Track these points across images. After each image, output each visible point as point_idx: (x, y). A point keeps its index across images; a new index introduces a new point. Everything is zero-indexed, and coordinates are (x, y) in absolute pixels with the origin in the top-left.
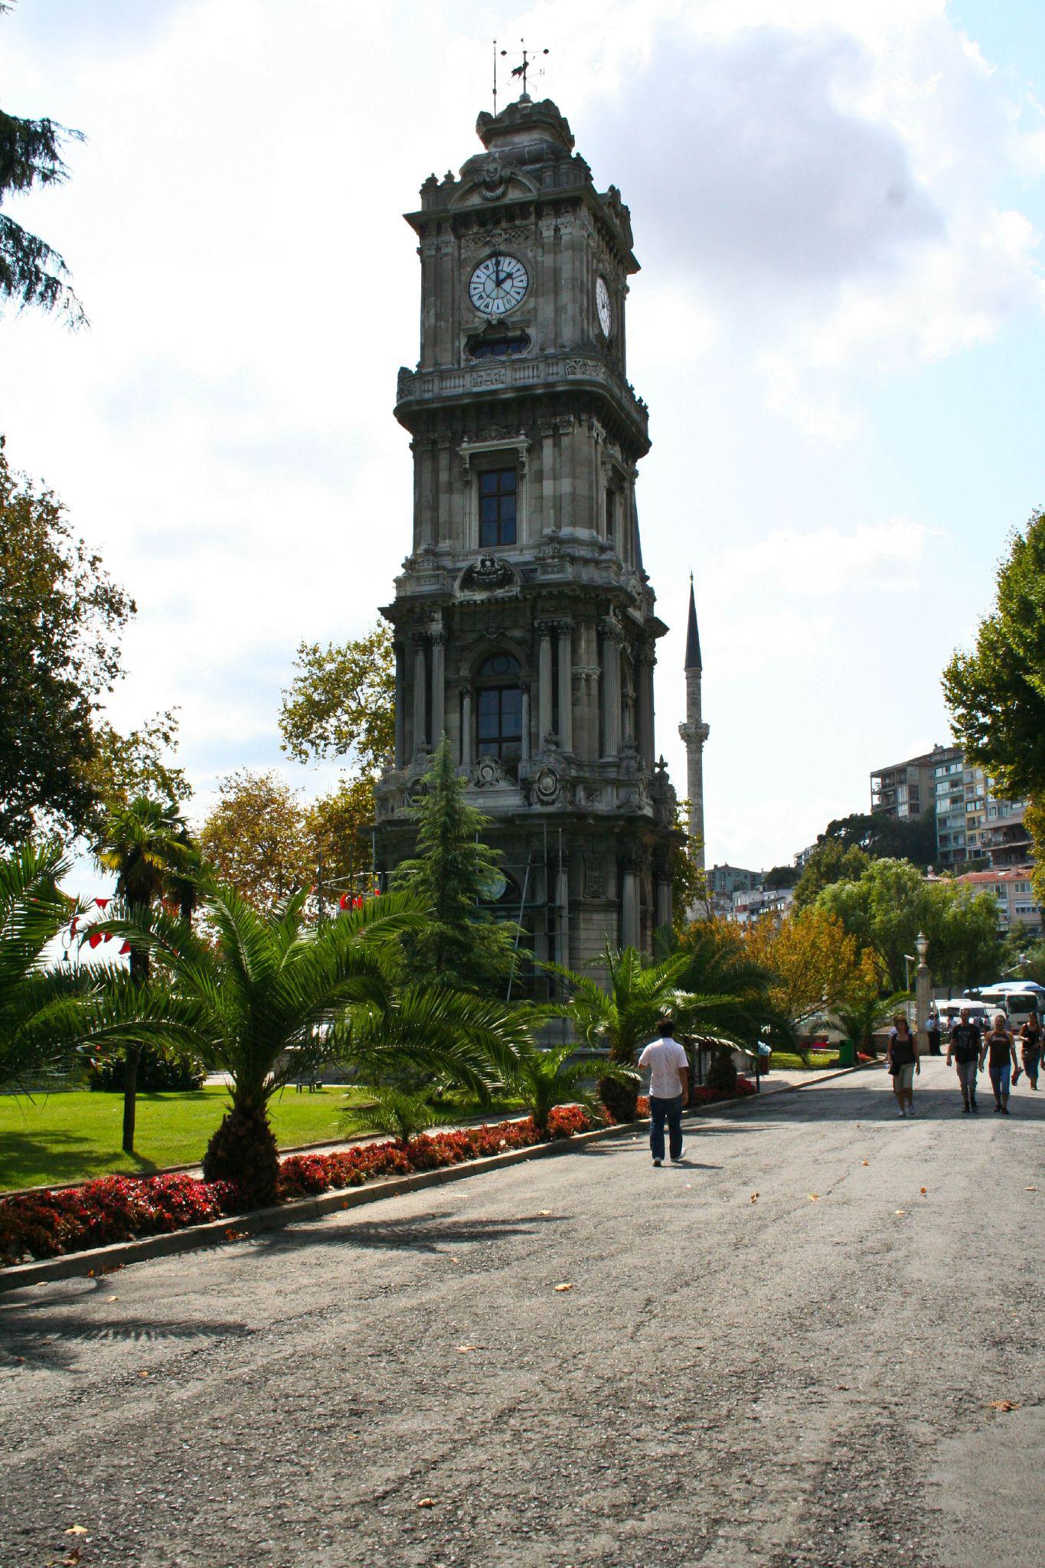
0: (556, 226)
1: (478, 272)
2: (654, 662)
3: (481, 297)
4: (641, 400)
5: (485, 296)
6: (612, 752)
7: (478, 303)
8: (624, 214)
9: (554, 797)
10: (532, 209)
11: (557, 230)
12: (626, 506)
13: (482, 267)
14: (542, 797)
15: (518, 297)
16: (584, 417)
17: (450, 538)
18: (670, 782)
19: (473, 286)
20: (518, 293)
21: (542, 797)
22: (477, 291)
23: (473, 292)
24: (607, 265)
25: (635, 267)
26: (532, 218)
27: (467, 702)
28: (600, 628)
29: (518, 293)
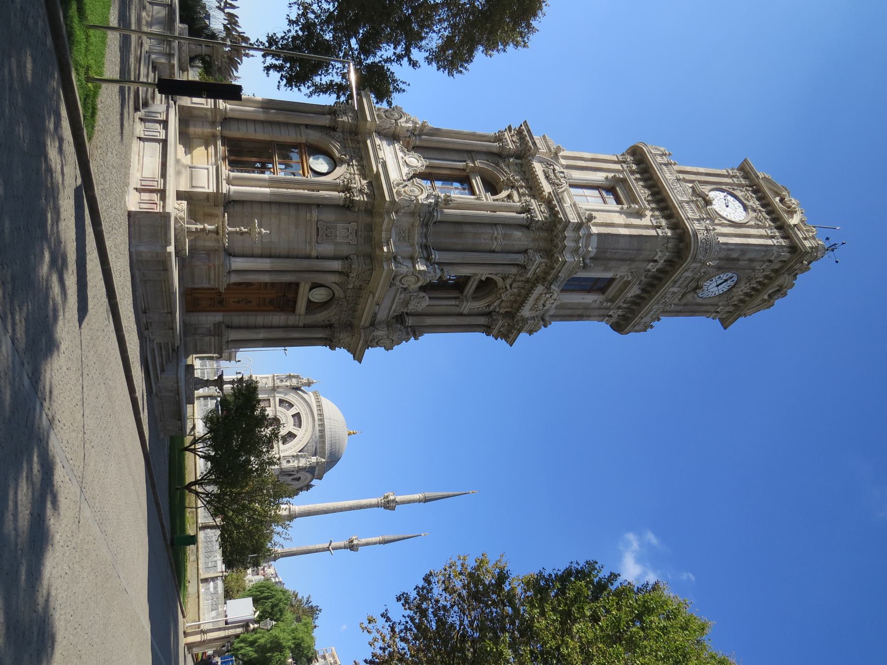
0: (776, 236)
4: (659, 320)
5: (718, 198)
8: (768, 303)
16: (670, 245)
18: (404, 342)
23: (717, 192)
24: (744, 288)
25: (725, 323)
27: (461, 165)
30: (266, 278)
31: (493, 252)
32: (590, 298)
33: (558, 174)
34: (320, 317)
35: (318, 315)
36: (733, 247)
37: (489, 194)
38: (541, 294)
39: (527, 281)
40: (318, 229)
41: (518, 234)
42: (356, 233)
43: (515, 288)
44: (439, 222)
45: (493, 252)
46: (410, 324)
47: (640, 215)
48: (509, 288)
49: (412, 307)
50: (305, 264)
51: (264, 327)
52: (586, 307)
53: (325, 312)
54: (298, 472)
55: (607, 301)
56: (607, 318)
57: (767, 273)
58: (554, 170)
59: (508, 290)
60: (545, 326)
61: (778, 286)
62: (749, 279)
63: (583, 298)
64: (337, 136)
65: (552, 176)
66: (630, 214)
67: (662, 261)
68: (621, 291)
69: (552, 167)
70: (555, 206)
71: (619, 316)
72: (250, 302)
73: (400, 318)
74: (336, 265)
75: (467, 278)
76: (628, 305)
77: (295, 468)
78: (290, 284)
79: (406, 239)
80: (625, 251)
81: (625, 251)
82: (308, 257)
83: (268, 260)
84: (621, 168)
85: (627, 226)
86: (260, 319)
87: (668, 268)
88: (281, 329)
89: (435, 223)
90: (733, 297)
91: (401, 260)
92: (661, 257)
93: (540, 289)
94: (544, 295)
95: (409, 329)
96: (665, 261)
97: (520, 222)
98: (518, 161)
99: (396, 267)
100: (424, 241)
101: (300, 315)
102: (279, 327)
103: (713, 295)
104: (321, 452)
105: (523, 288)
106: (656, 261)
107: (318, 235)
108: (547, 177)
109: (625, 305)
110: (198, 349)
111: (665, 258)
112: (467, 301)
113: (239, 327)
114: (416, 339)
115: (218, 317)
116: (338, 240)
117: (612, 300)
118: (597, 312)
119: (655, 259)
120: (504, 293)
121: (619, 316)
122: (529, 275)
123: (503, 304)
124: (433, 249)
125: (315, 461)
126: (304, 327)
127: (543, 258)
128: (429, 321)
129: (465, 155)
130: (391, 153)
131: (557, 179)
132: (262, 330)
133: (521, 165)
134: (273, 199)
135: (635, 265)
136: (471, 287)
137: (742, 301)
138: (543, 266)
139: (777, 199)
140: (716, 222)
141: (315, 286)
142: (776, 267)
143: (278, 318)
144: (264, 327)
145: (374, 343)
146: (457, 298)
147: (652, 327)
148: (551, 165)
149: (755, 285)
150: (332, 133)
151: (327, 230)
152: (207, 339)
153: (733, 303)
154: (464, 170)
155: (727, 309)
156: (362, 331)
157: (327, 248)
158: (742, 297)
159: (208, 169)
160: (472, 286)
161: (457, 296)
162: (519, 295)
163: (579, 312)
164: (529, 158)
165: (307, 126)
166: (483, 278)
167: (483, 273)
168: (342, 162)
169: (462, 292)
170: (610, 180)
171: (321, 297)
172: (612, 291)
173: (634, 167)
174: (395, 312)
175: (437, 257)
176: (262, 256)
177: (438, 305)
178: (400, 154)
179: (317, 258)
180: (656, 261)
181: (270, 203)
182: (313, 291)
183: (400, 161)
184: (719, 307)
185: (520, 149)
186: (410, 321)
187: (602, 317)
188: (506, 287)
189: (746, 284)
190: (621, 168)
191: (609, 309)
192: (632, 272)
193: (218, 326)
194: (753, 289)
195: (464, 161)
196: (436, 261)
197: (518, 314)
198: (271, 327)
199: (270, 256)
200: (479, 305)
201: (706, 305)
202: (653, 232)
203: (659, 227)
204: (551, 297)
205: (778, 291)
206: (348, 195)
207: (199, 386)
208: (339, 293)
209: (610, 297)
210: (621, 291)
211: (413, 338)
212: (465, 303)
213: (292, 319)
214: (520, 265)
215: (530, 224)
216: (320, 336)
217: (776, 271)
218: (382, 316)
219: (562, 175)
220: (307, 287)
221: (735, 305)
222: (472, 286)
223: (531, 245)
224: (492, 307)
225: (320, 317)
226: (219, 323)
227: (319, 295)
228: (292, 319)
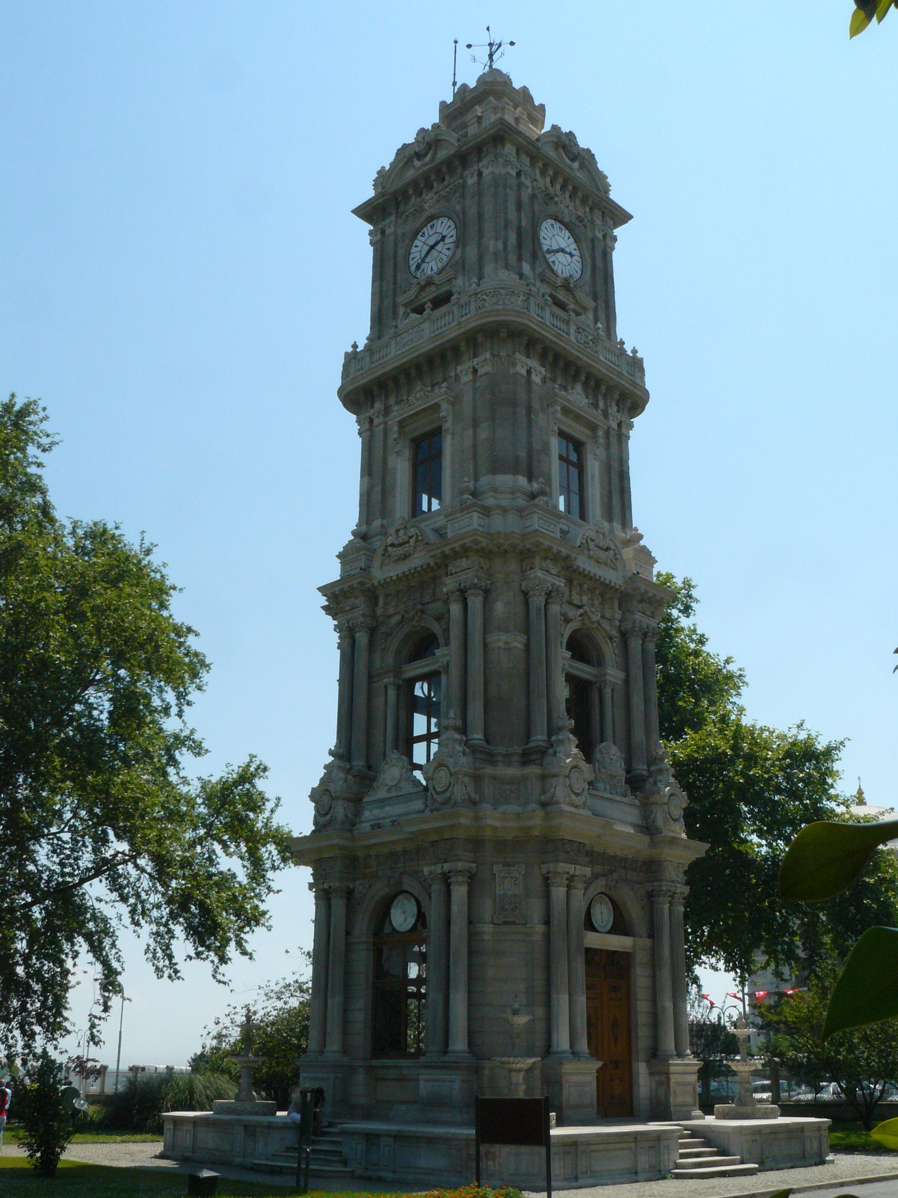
1: (416, 242)
4: (622, 343)
8: (586, 159)
9: (448, 794)
10: (457, 163)
11: (480, 174)
12: (609, 458)
13: (419, 237)
14: (435, 796)
17: (383, 517)
19: (411, 256)
20: (449, 249)
21: (435, 796)
22: (415, 260)
23: (411, 263)
26: (459, 170)
27: (392, 692)
28: (523, 588)
29: (449, 249)
30: (582, 1000)
32: (594, 467)
37: (438, 652)
38: (590, 557)
39: (570, 582)
40: (505, 923)
42: (508, 865)
43: (581, 600)
44: (485, 736)
46: (645, 767)
48: (581, 611)
52: (607, 468)
55: (595, 437)
57: (538, 172)
58: (393, 545)
59: (586, 612)
60: (641, 537)
61: (556, 149)
62: (549, 198)
63: (593, 477)
65: (401, 551)
67: (529, 361)
68: (578, 418)
70: (453, 549)
71: (618, 411)
75: (570, 679)
76: (600, 398)
78: (588, 963)
86: (642, 1006)
87: (539, 348)
89: (487, 741)
90: (578, 217)
94: (591, 552)
95: (653, 768)
96: (528, 357)
98: (381, 600)
100: (515, 758)
102: (654, 978)
105: (581, 586)
106: (529, 372)
107: (514, 923)
108: (405, 557)
109: (601, 404)
117: (593, 428)
118: (614, 450)
119: (526, 374)
120: (589, 618)
121: (618, 411)
122: (561, 583)
123: (608, 615)
124: (528, 743)
126: (651, 936)
131: (408, 542)
135: (536, 405)
136: (582, 671)
137: (584, 201)
138: (549, 564)
139: (417, 163)
141: (590, 926)
142: (528, 160)
143: (641, 979)
146: (600, 691)
147: (635, 351)
149: (558, 187)
151: (507, 910)
153: (588, 215)
154: (399, 687)
155: (598, 222)
158: (578, 202)
160: (584, 671)
161: (596, 691)
162: (592, 591)
164: (376, 584)
165: (348, 933)
166: (568, 654)
167: (562, 657)
171: (605, 911)
172: (579, 432)
173: (378, 405)
175: (540, 737)
176: (548, 1005)
177: (613, 721)
178: (382, 794)
180: (529, 372)
182: (596, 926)
183: (393, 794)
184: (595, 237)
185: (362, 598)
187: (621, 437)
188: (581, 615)
189: (556, 203)
191: (607, 433)
192: (548, 406)
194: (563, 187)
195: (386, 688)
196: (546, 738)
197: (623, 589)
200: (610, 651)
201: (593, 259)
204: (593, 541)
205: (564, 147)
208: (599, 885)
210: (578, 418)
212: (608, 678)
213: (641, 957)
214: (546, 600)
215: (482, 590)
217: (533, 159)
219: (401, 532)
221: (591, 209)
222: (584, 671)
224: (614, 633)
227: (603, 915)
228: (641, 957)
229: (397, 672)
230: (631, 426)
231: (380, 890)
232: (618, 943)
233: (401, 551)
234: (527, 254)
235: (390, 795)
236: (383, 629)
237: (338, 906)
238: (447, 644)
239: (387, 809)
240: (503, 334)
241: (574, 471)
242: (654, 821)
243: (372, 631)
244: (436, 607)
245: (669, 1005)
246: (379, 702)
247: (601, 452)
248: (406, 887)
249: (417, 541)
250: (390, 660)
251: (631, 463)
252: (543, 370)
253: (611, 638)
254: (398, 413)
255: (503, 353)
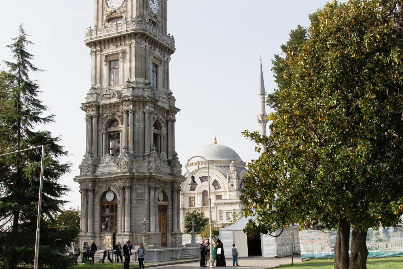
2: (175, 120)
3: (110, 3)
5: (111, 3)
6: (147, 153)
7: (109, 5)
12: (164, 69)
15: (121, 2)
27: (104, 136)
30: (157, 218)
31: (145, 127)
32: (160, 72)
33: (108, 93)
34: (169, 195)
35: (168, 196)
36: (138, 4)
40: (139, 199)
41: (137, 116)
42: (140, 185)
45: (145, 127)
47: (124, 52)
48: (157, 116)
49: (166, 159)
50: (152, 204)
51: (172, 217)
52: (164, 73)
53: (167, 194)
54: (239, 179)
55: (161, 64)
56: (168, 60)
58: (105, 94)
60: (172, 93)
64: (97, 190)
65: (109, 96)
66: (124, 57)
67: (146, 43)
69: (104, 95)
72: (163, 223)
73: (169, 162)
74: (152, 192)
76: (163, 51)
77: (236, 181)
78: (159, 208)
79: (141, 165)
80: (142, 63)
81: (142, 63)
82: (150, 202)
83: (151, 218)
84: (99, 55)
85: (130, 61)
86: (170, 219)
88: (173, 211)
89: (134, 152)
91: (150, 167)
92: (144, 44)
93: (159, 103)
95: (174, 158)
96: (146, 42)
97: (132, 115)
98: (101, 109)
99: (153, 169)
100: (141, 157)
101: (168, 204)
103: (158, 6)
104: (227, 164)
105: (157, 109)
106: (146, 47)
109: (163, 54)
110: (180, 242)
111: (145, 43)
112: (162, 132)
113: (173, 227)
114: (177, 155)
115: (169, 235)
116: (143, 192)
117: (161, 61)
118: (166, 67)
122: (153, 109)
124: (144, 153)
125: (233, 167)
127: (147, 105)
128: (170, 149)
129: (100, 133)
130: (104, 168)
132: (174, 218)
133: (102, 108)
134: (129, 216)
135: (147, 56)
136: (156, 131)
140: (125, 9)
144: (172, 217)
145: (179, 173)
146: (160, 137)
147: (172, 36)
148: (103, 95)
150: (96, 191)
152: (177, 238)
154: (106, 134)
156: (175, 179)
157: (146, 196)
159: (119, 239)
160: (157, 132)
163: (166, 76)
164: (100, 105)
168: (109, 188)
169: (158, 135)
170: (106, 63)
172: (157, 62)
173: (98, 48)
174: (167, 166)
175: (148, 152)
176: (150, 220)
178: (104, 164)
179: (150, 199)
180: (146, 47)
181: (131, 217)
183: (107, 165)
185: (95, 108)
186: (170, 158)
190: (99, 55)
191: (164, 63)
193: (172, 235)
195: (102, 134)
196: (149, 152)
198: (172, 214)
199: (150, 217)
201: (162, 5)
202: (133, 49)
203: (130, 45)
206: (127, 188)
207: (194, 242)
209: (160, 63)
211: (177, 156)
212: (163, 133)
213: (170, 207)
216: (176, 195)
218: (168, 170)
219: (108, 91)
220: (159, 202)
223: (141, 110)
224: (165, 121)
225: (169, 195)
226: (171, 234)
228: (170, 207)
229: (106, 130)
230: (170, 59)
231: (104, 190)
232: (165, 203)
233: (109, 96)
234: (145, 7)
235: (106, 165)
236: (102, 117)
237: (90, 194)
238: (122, 124)
239: (105, 169)
240: (139, 35)
241: (155, 74)
242: (174, 172)
243: (98, 117)
244: (119, 114)
245: (176, 219)
246: (101, 138)
247: (162, 68)
248: (111, 190)
249: (113, 94)
250: (104, 127)
251: (170, 70)
252: (149, 45)
253: (164, 122)
254: (105, 52)
255: (139, 41)
